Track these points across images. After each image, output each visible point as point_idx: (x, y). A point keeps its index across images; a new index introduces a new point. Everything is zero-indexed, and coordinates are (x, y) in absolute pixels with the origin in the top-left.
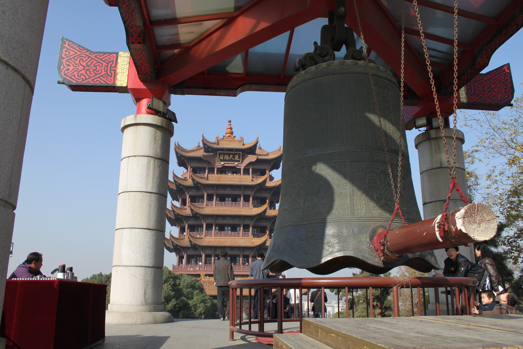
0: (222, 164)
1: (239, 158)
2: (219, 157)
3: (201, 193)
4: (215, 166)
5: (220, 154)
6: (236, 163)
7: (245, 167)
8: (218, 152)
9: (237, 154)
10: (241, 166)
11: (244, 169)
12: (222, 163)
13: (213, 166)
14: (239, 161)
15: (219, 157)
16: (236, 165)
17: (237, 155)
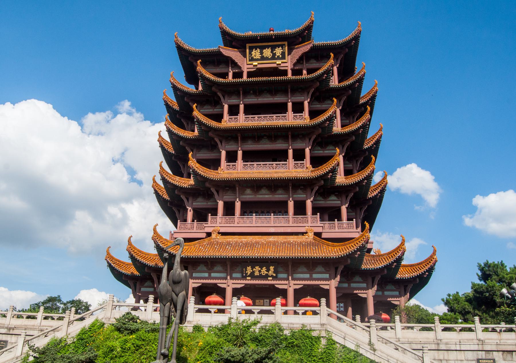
0: (254, 66)
1: (283, 54)
2: (250, 53)
3: (220, 110)
4: (244, 69)
5: (251, 49)
6: (279, 62)
7: (295, 65)
8: (248, 45)
9: (279, 46)
10: (287, 67)
11: (293, 70)
12: (255, 63)
13: (240, 68)
14: (283, 57)
15: (250, 53)
16: (277, 65)
17: (279, 48)
